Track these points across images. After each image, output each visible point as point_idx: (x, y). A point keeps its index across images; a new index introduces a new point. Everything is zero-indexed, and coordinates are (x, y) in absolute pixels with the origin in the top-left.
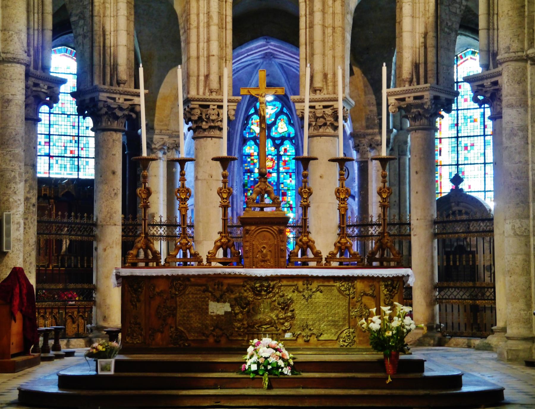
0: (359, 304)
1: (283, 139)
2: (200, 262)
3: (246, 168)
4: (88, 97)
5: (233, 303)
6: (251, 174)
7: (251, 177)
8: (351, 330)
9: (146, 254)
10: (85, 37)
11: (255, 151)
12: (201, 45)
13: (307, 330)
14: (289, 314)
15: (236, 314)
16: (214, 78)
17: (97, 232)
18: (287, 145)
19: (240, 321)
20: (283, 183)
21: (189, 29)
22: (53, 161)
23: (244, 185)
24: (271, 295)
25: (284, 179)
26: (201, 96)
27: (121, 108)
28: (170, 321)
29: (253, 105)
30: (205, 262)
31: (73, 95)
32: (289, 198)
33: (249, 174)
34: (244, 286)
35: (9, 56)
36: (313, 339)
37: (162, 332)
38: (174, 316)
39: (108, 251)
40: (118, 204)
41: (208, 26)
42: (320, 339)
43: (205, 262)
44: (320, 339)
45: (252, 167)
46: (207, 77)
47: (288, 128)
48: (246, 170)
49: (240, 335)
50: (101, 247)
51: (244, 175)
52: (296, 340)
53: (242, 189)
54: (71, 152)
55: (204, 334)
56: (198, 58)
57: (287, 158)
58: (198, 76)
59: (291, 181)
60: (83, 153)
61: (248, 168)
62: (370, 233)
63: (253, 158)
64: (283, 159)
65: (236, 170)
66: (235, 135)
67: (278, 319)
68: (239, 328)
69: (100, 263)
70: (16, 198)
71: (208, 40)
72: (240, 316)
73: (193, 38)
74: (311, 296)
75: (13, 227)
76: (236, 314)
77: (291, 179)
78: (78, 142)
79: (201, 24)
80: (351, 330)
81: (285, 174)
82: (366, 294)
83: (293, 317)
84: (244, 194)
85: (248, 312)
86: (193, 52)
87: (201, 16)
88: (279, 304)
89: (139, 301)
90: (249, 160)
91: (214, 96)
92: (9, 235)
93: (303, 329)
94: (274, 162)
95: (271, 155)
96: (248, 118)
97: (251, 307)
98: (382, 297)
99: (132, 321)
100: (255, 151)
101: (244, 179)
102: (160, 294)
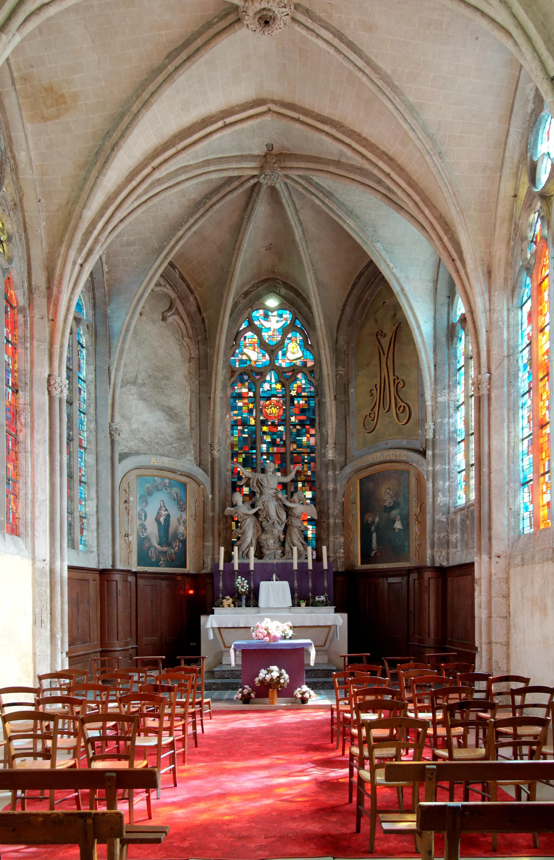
1: (294, 370)
3: (235, 418)
6: (244, 428)
7: (244, 432)
11: (250, 390)
18: (301, 380)
20: (294, 443)
23: (232, 446)
25: (298, 435)
29: (246, 315)
32: (305, 466)
33: (240, 428)
45: (245, 415)
47: (303, 352)
48: (235, 421)
51: (232, 429)
53: (230, 451)
57: (302, 402)
59: (308, 440)
61: (239, 418)
62: (445, 520)
63: (246, 401)
64: (296, 402)
65: (218, 416)
66: (215, 357)
77: (308, 435)
81: (298, 427)
84: (232, 460)
90: (240, 404)
94: (280, 408)
95: (275, 396)
96: (237, 336)
100: (250, 390)
101: (232, 435)
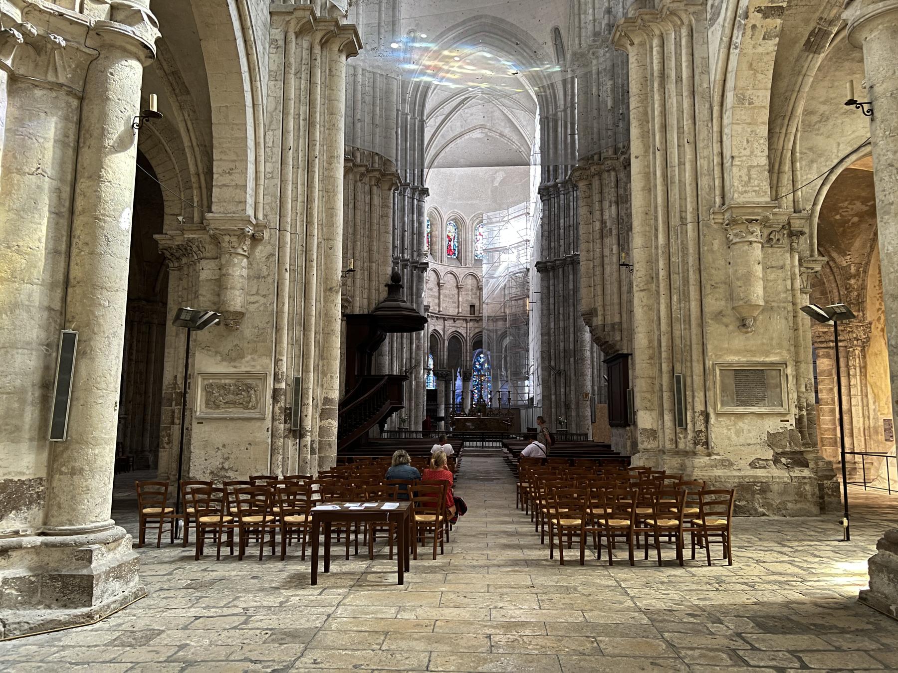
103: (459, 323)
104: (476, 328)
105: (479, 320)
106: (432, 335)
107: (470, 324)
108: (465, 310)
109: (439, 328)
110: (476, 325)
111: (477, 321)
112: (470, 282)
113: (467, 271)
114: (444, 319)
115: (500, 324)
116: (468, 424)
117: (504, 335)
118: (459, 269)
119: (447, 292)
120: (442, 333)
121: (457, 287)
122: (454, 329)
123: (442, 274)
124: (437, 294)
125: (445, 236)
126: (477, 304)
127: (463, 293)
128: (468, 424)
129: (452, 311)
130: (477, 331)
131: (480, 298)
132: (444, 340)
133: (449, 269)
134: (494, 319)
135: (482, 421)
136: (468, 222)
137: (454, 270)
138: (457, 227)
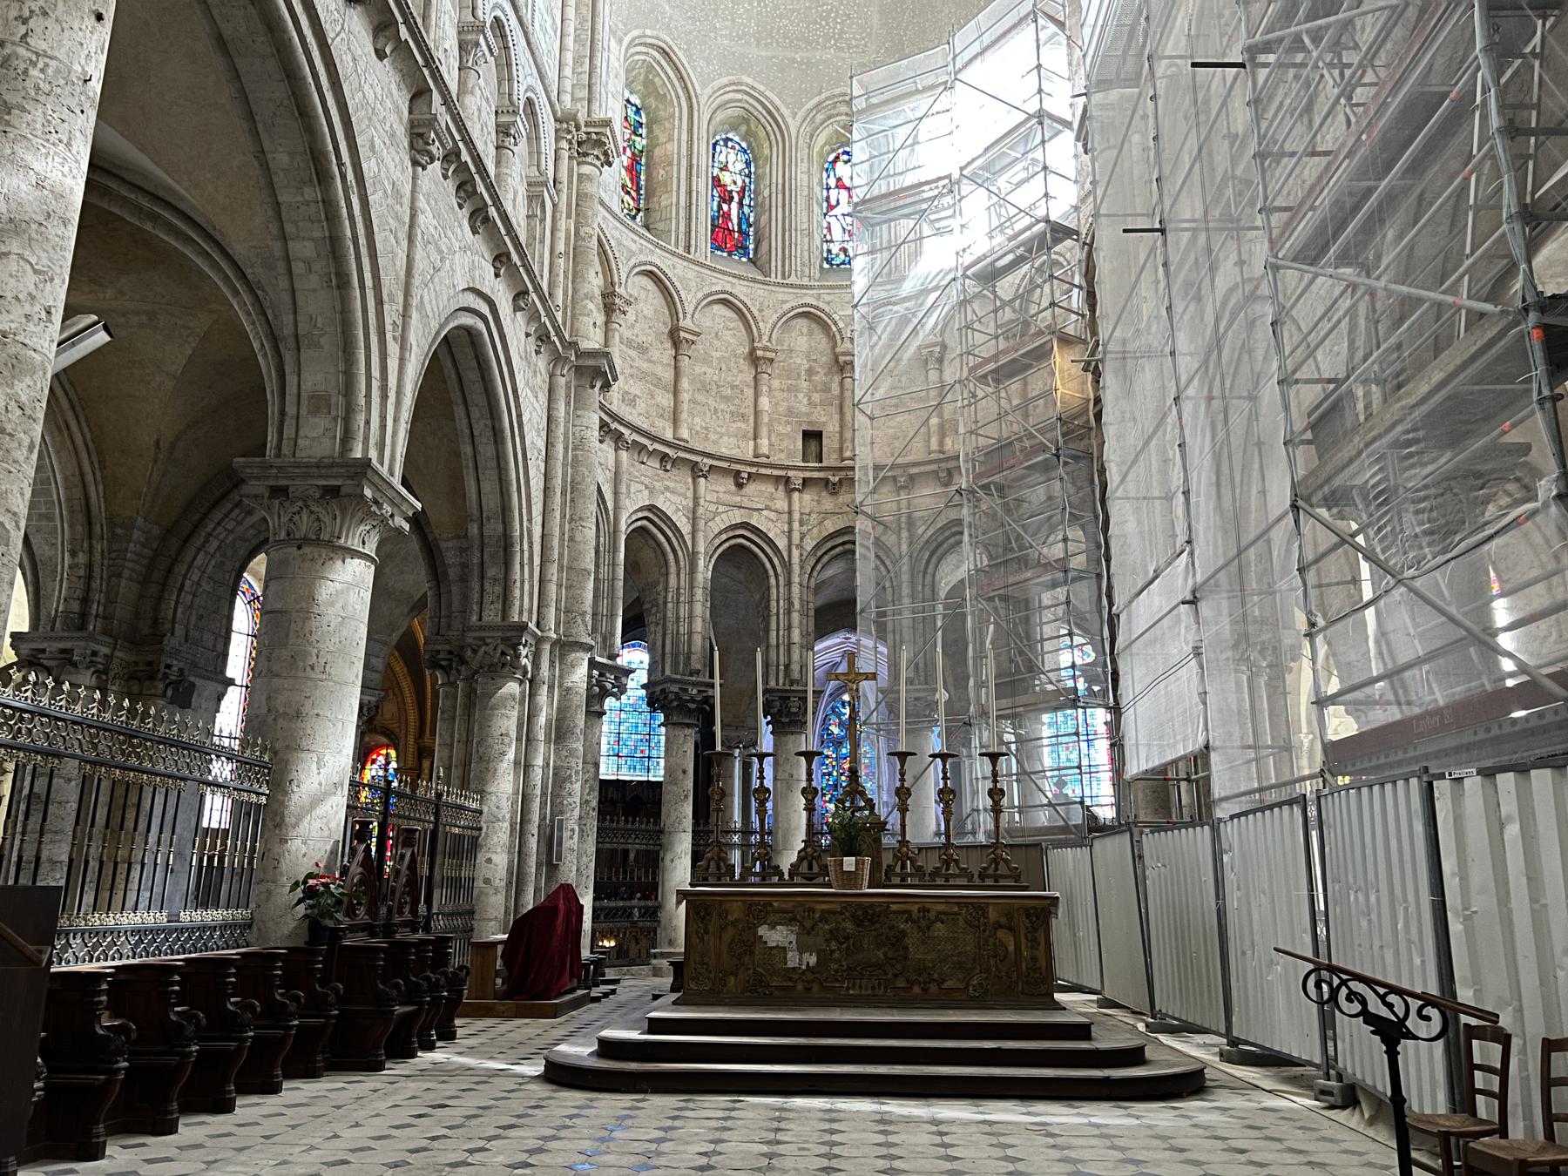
0: (991, 940)
2: (781, 875)
4: (658, 689)
5: (828, 936)
8: (984, 975)
9: (718, 868)
10: (657, 624)
12: (781, 633)
13: (925, 975)
14: (901, 953)
15: (832, 952)
16: (795, 667)
17: (664, 839)
19: (838, 961)
21: (769, 616)
22: (622, 761)
24: (878, 925)
26: (781, 687)
27: (693, 700)
28: (746, 960)
30: (786, 877)
31: (643, 686)
34: (842, 914)
35: (570, 639)
36: (933, 987)
37: (736, 976)
38: (752, 953)
39: (677, 862)
40: (688, 809)
41: (789, 612)
42: (945, 986)
43: (786, 877)
44: (945, 986)
46: (787, 666)
49: (837, 981)
50: (668, 857)
52: (911, 988)
54: (642, 752)
55: (790, 979)
56: (778, 646)
58: (778, 666)
60: (654, 753)
67: (887, 958)
68: (836, 971)
69: (666, 876)
70: (570, 800)
71: (789, 628)
72: (836, 955)
73: (773, 626)
74: (928, 928)
75: (566, 834)
76: (832, 952)
78: (649, 741)
79: (781, 611)
80: (984, 975)
82: (1001, 927)
83: (906, 958)
85: (848, 948)
86: (773, 641)
87: (781, 602)
88: (888, 938)
89: (707, 932)
91: (795, 687)
92: (560, 844)
93: (920, 974)
97: (851, 941)
98: (1023, 931)
99: (698, 959)
102: (734, 923)
103: (757, 492)
104: (828, 514)
105: (837, 482)
106: (639, 535)
107: (805, 501)
108: (785, 448)
109: (674, 505)
110: (828, 503)
111: (832, 488)
112: (802, 343)
113: (792, 299)
114: (696, 471)
115: (927, 497)
116: (775, 936)
117: (945, 541)
118: (760, 291)
119: (711, 373)
120: (685, 527)
121: (754, 359)
122: (737, 517)
123: (689, 299)
124: (668, 375)
125: (702, 185)
126: (831, 430)
127: (774, 382)
128: (775, 936)
129: (731, 444)
130: (831, 526)
131: (843, 405)
132: (693, 557)
133: (721, 284)
134: (899, 477)
135: (868, 915)
136: (793, 125)
137: (741, 290)
138: (753, 157)
